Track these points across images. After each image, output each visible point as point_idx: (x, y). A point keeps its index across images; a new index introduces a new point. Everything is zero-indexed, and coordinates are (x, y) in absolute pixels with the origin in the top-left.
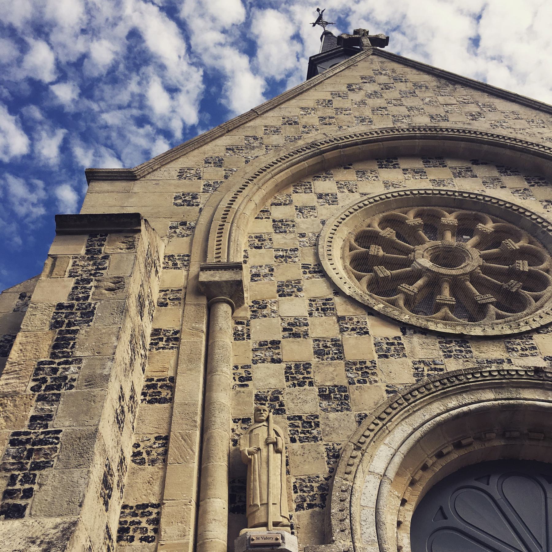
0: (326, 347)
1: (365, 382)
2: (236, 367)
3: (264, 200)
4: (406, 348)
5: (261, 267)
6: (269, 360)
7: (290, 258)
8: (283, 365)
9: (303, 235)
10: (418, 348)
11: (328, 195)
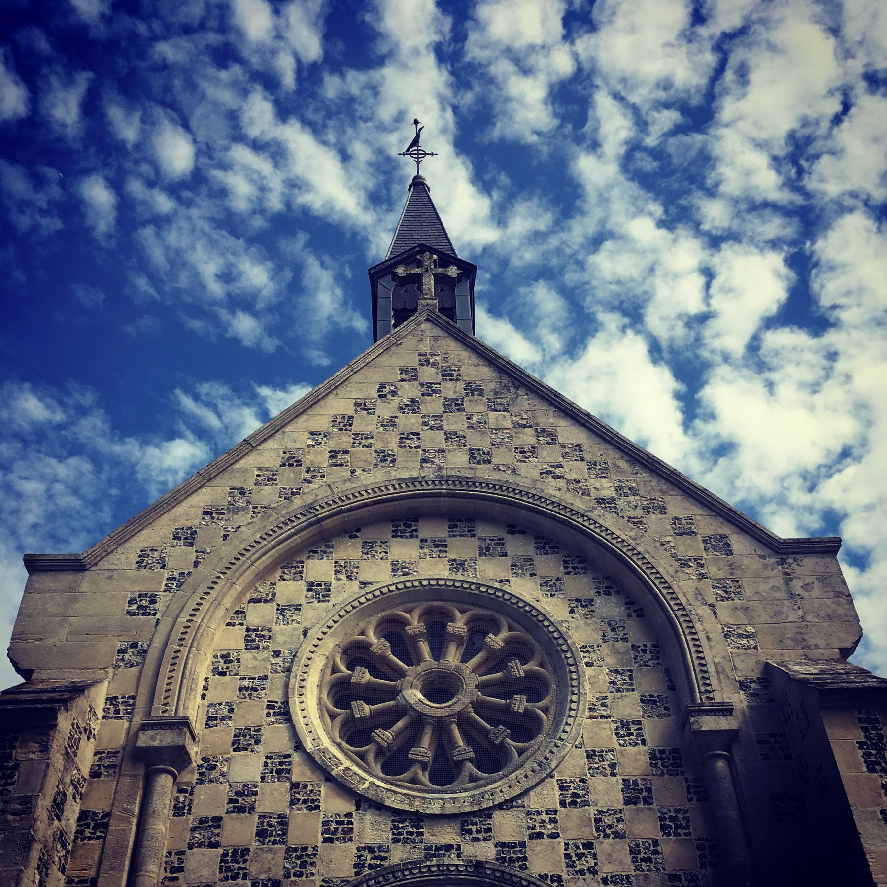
0: (270, 826)
2: (170, 853)
3: (239, 598)
4: (355, 830)
5: (220, 704)
6: (206, 844)
7: (256, 690)
8: (221, 851)
9: (277, 654)
10: (368, 829)
11: (319, 585)
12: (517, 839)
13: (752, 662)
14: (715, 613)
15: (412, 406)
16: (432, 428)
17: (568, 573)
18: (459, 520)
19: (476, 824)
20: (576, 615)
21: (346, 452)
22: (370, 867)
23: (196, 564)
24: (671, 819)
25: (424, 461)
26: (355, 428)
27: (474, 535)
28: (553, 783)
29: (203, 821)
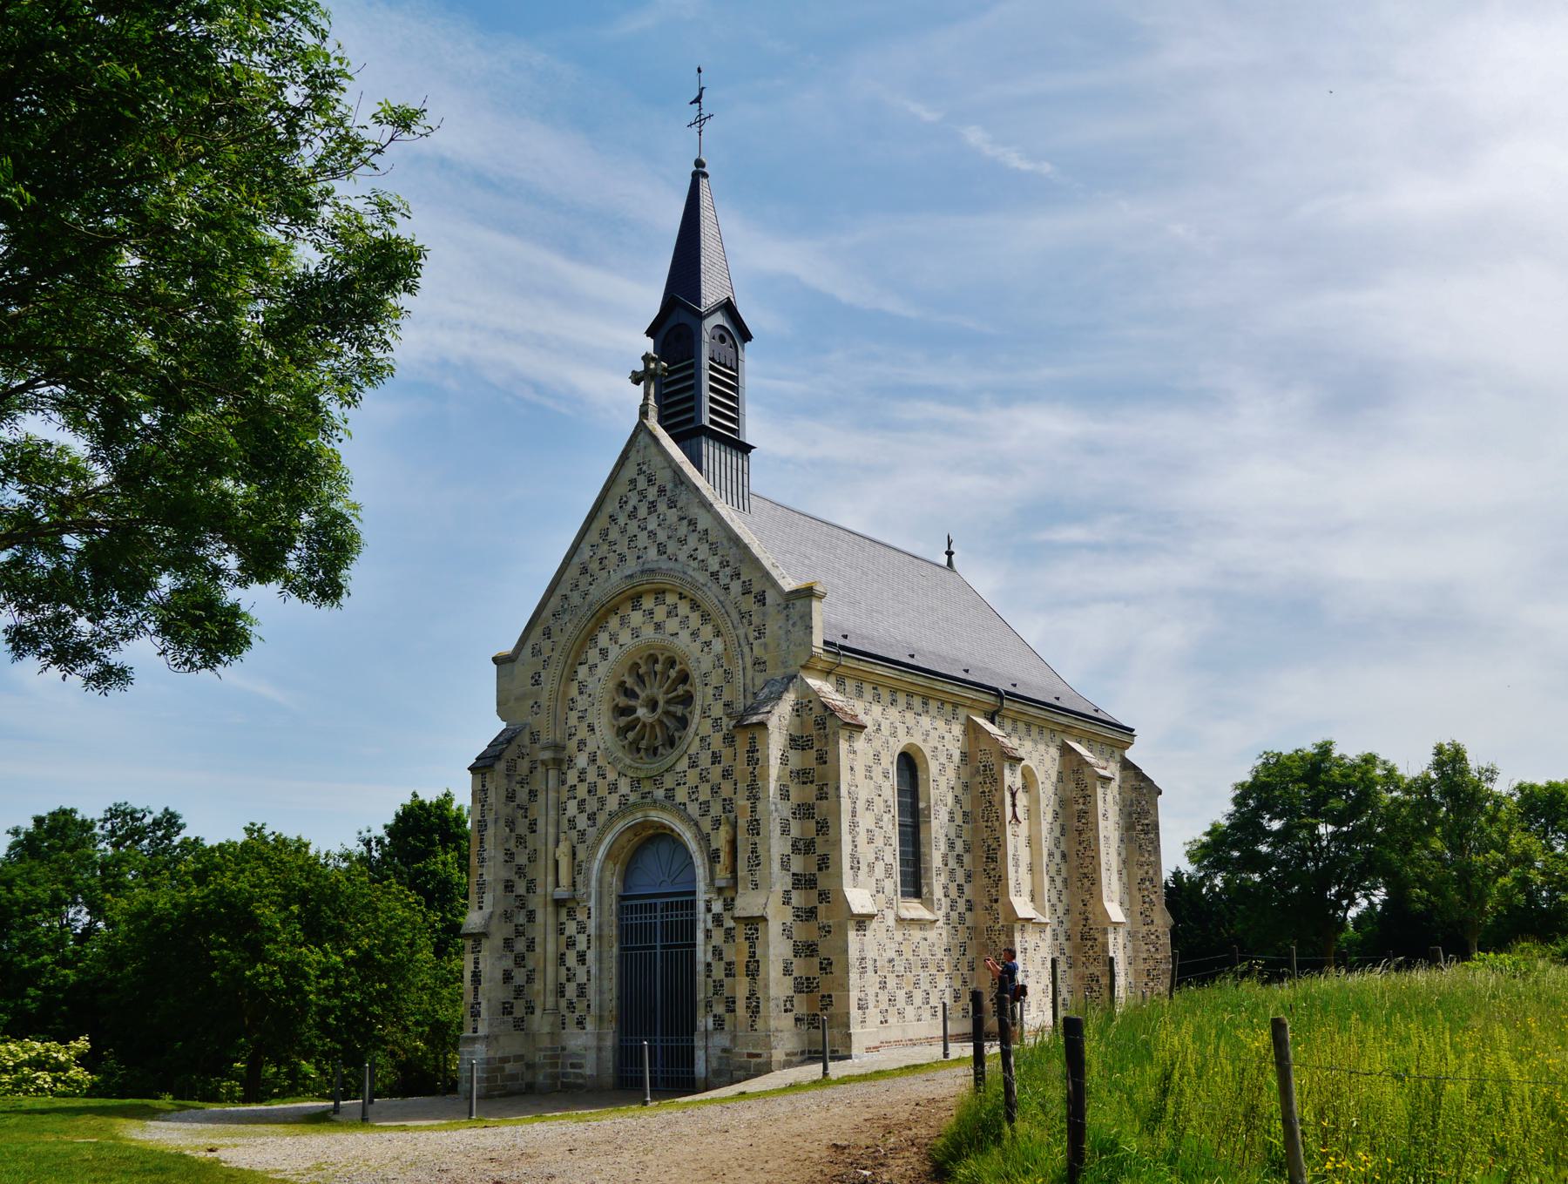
3: (572, 665)
15: (633, 515)
24: (727, 771)
25: (638, 558)
28: (686, 758)
29: (571, 787)
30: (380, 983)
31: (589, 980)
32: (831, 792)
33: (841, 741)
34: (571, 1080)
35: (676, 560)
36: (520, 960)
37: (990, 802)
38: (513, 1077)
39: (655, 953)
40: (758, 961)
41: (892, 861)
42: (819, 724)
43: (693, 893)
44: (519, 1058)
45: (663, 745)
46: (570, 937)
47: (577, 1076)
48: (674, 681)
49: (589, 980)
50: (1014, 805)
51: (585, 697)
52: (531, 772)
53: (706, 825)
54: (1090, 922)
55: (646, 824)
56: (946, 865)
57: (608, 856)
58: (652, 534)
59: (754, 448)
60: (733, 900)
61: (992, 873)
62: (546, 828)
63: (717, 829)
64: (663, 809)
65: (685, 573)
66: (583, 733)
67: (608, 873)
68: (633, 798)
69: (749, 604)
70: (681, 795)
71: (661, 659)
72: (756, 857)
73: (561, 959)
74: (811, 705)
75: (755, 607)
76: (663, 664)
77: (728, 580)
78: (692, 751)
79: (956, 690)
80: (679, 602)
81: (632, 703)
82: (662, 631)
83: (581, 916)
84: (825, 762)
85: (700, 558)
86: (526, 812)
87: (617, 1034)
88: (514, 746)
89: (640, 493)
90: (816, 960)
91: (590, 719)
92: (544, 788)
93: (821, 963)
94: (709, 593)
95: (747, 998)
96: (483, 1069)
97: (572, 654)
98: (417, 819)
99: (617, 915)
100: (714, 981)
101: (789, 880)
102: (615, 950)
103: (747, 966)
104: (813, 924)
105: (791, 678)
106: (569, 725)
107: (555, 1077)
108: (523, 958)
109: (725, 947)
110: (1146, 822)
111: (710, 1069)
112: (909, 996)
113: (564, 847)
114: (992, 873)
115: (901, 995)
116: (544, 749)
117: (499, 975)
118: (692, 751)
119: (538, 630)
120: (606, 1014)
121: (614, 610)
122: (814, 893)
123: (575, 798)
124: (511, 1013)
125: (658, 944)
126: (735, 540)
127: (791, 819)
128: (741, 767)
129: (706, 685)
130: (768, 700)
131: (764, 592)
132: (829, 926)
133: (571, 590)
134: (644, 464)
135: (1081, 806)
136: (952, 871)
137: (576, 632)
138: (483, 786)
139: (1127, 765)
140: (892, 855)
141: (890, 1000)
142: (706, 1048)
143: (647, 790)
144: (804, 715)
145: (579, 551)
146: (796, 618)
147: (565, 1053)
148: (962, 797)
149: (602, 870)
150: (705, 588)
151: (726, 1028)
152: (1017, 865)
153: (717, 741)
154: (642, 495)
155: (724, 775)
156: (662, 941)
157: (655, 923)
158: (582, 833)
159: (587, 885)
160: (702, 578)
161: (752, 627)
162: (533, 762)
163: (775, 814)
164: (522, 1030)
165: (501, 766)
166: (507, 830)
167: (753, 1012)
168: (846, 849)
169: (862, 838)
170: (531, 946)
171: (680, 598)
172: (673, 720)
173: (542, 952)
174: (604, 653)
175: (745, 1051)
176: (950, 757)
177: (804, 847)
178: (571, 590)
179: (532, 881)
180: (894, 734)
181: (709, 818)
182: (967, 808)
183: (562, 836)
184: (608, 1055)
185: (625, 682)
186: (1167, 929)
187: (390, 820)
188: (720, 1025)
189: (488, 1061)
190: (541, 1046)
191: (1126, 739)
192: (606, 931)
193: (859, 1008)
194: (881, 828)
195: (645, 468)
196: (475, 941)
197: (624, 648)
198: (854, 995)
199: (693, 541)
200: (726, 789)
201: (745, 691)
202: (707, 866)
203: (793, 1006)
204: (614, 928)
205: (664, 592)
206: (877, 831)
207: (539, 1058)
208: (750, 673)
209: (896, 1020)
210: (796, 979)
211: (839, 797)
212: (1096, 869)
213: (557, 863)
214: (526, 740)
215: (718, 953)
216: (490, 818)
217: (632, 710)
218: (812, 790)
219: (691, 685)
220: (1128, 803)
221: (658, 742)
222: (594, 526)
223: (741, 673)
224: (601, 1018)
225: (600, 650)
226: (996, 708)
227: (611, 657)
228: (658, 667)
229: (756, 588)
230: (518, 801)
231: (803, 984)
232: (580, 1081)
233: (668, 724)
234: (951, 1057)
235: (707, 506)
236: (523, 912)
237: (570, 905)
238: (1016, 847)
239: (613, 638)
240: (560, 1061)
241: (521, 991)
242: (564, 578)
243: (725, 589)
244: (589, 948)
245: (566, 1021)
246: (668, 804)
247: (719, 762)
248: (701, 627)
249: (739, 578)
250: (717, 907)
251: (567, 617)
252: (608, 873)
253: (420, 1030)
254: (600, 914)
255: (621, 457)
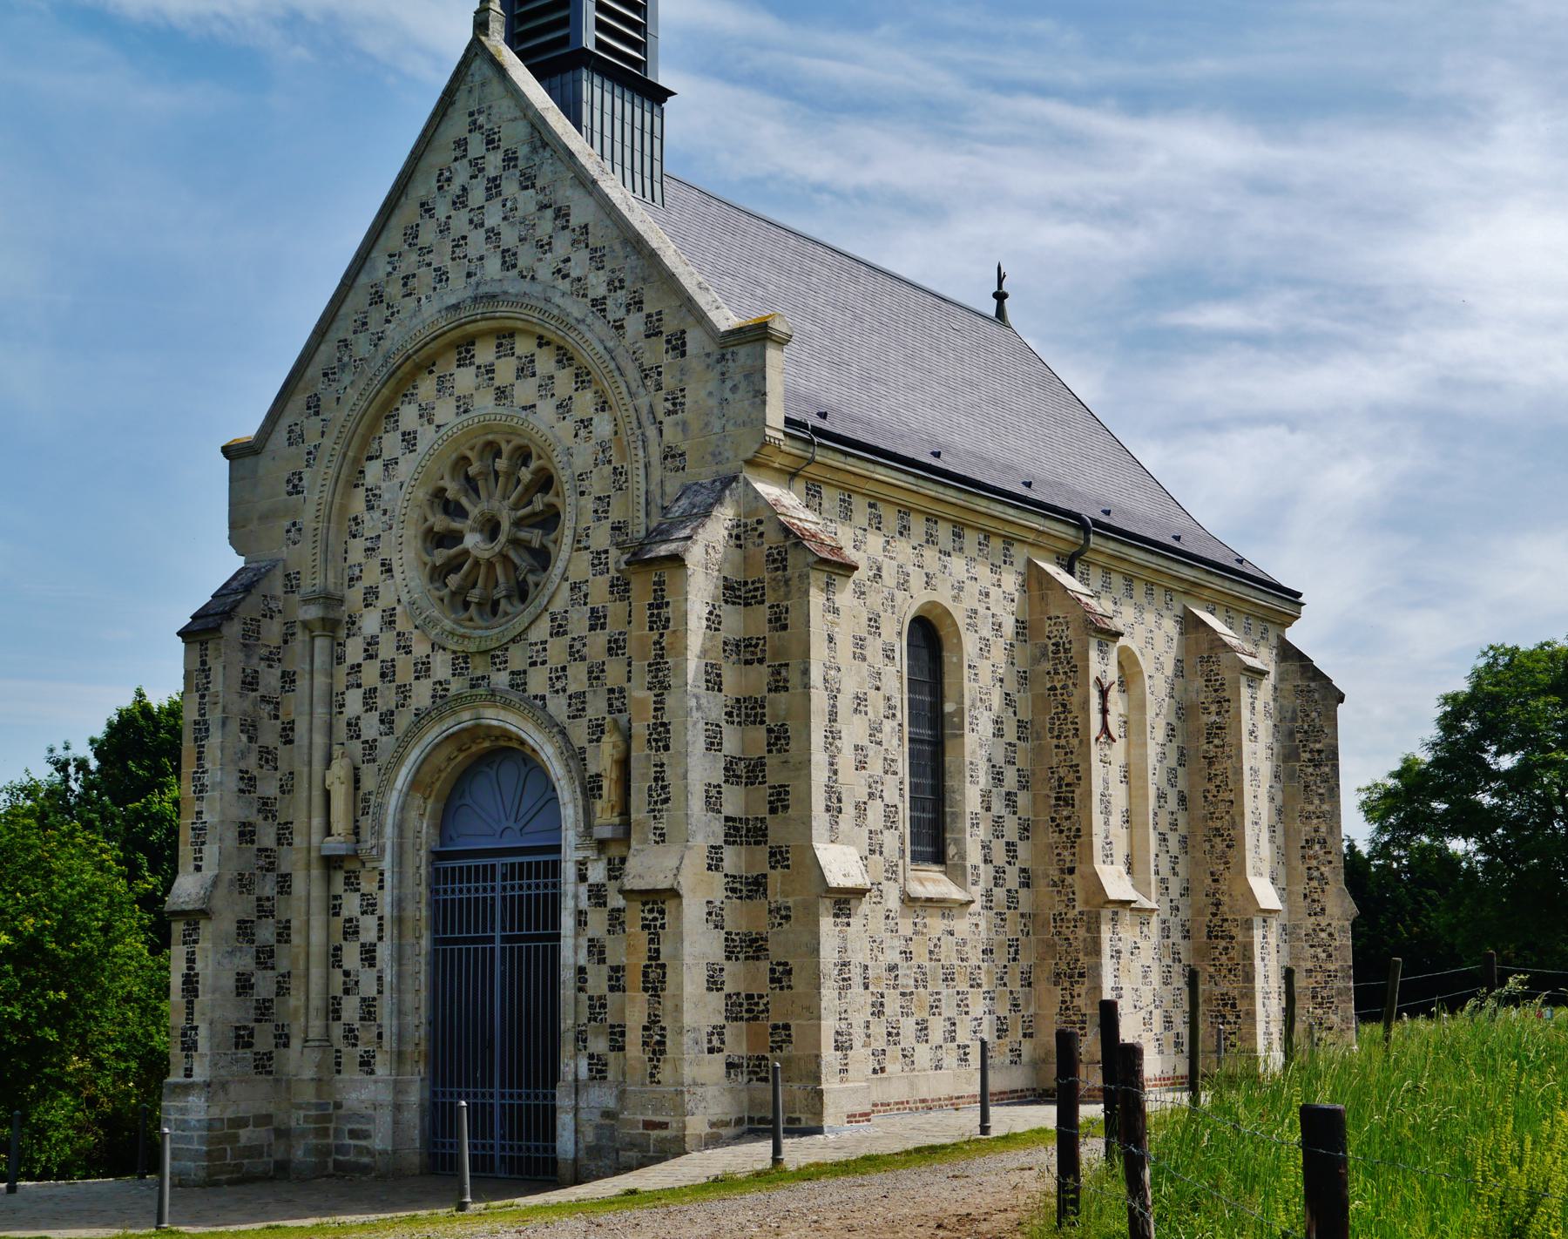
1: (403, 706)
3: (356, 461)
7: (373, 550)
8: (362, 690)
12: (521, 669)
13: (677, 485)
14: (661, 431)
15: (460, 202)
16: (476, 227)
17: (577, 390)
18: (504, 337)
19: (498, 657)
20: (578, 440)
21: (414, 276)
22: (441, 697)
23: (323, 433)
24: (616, 641)
25: (469, 275)
26: (421, 242)
27: (513, 354)
28: (546, 617)
29: (352, 667)
30: (57, 991)
31: (380, 992)
32: (794, 678)
33: (813, 591)
34: (351, 1157)
35: (533, 278)
36: (265, 957)
37: (1064, 706)
38: (254, 1151)
39: (492, 949)
40: (663, 966)
41: (896, 800)
42: (774, 561)
43: (557, 849)
44: (264, 1120)
45: (508, 597)
46: (350, 920)
47: (361, 1151)
48: (527, 489)
49: (380, 992)
50: (1104, 711)
51: (377, 514)
52: (286, 642)
53: (579, 733)
54: (1224, 908)
55: (476, 732)
56: (988, 809)
57: (415, 784)
58: (493, 235)
59: (673, 94)
60: (623, 860)
61: (1066, 824)
62: (311, 734)
63: (598, 740)
64: (507, 705)
65: (548, 300)
66: (372, 575)
67: (413, 814)
68: (456, 686)
69: (656, 353)
70: (538, 682)
71: (506, 449)
72: (663, 788)
73: (334, 957)
74: (761, 528)
75: (667, 359)
76: (510, 458)
77: (621, 313)
78: (557, 606)
79: (1011, 514)
80: (537, 351)
81: (456, 525)
82: (507, 402)
83: (367, 886)
84: (785, 627)
85: (574, 274)
86: (277, 709)
87: (427, 1082)
88: (254, 598)
89: (474, 163)
90: (764, 966)
91: (384, 552)
92: (307, 667)
93: (773, 971)
94: (588, 335)
95: (645, 1028)
96: (201, 1137)
97: (355, 444)
98: (139, 731)
99: (429, 885)
100: (591, 998)
101: (718, 829)
102: (425, 943)
103: (645, 974)
104: (760, 905)
105: (729, 481)
106: (351, 561)
107: (323, 1152)
108: (271, 954)
109: (609, 941)
110: (1318, 746)
111: (581, 1146)
112: (923, 1027)
113: (340, 769)
114: (1066, 824)
115: (908, 1026)
116: (306, 601)
117: (229, 982)
118: (557, 606)
119: (299, 400)
120: (409, 1048)
121: (428, 366)
122: (762, 852)
123: (359, 686)
124: (249, 1045)
125: (498, 934)
126: (636, 243)
127: (723, 724)
128: (639, 632)
129: (582, 493)
130: (686, 518)
131: (683, 332)
132: (788, 908)
133: (355, 332)
134: (480, 112)
135: (1214, 718)
136: (998, 821)
137: (363, 404)
138: (203, 663)
139: (1288, 653)
140: (897, 791)
141: (889, 1034)
142: (576, 1110)
143: (479, 673)
144: (750, 546)
145: (368, 265)
146: (738, 377)
147: (342, 1112)
148: (1016, 697)
149: (403, 808)
150: (582, 327)
151: (610, 1076)
152: (1107, 812)
153: (599, 590)
154: (477, 167)
155: (610, 649)
156: (503, 929)
157: (493, 899)
158: (371, 746)
159: (379, 833)
160: (577, 309)
161: (662, 393)
162: (290, 624)
163: (696, 715)
164: (270, 1073)
165: (233, 630)
166: (244, 738)
167: (654, 1052)
168: (819, 776)
169: (846, 759)
170: (284, 934)
171: (540, 345)
172: (526, 556)
173: (303, 944)
174: (409, 439)
175: (641, 1118)
176: (998, 627)
177: (744, 772)
178: (355, 332)
179: (287, 825)
180: (903, 585)
181: (584, 722)
182: (1026, 715)
183: (337, 751)
184: (412, 1116)
185: (444, 490)
186: (1348, 924)
187: (100, 732)
188: (599, 1071)
189: (210, 1125)
190: (299, 1100)
191: (1287, 608)
192: (410, 912)
193: (837, 1048)
194: (880, 743)
195: (481, 119)
196: (188, 924)
197: (443, 430)
198: (829, 1026)
199: (562, 245)
200: (614, 673)
201: (647, 503)
202: (580, 803)
203: (723, 1042)
204: (423, 905)
205: (512, 335)
206: (872, 749)
207: (297, 1120)
208: (657, 473)
209: (898, 1067)
210: (729, 996)
211: (807, 686)
212: (1237, 822)
213: (327, 795)
214: (277, 586)
215: (596, 950)
216: (214, 717)
217: (457, 538)
218: (761, 674)
219: (557, 495)
220: (1289, 715)
221: (500, 593)
222: (394, 221)
223: (642, 472)
224: (400, 1057)
225: (404, 434)
226: (1076, 549)
227: (422, 446)
228: (501, 464)
229: (670, 326)
230: (262, 691)
231: (741, 1005)
232: (366, 1160)
233: (517, 561)
234: (994, 1133)
235: (588, 184)
236: (271, 877)
237: (348, 866)
238: (1106, 782)
239: (426, 414)
240: (332, 1126)
241: (268, 1008)
242: (343, 310)
243: (617, 328)
244: (380, 938)
245: (342, 1060)
246: (514, 697)
247: (603, 627)
248: (575, 395)
249: (640, 309)
250: (597, 873)
251: (347, 378)
252: (413, 814)
253: (123, 1065)
254: (400, 882)
255: (442, 100)
